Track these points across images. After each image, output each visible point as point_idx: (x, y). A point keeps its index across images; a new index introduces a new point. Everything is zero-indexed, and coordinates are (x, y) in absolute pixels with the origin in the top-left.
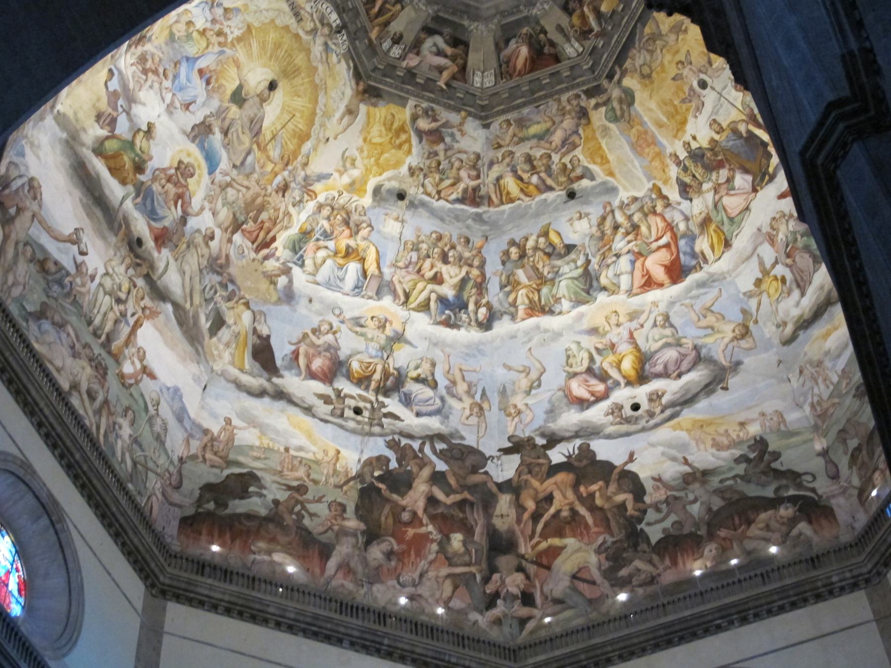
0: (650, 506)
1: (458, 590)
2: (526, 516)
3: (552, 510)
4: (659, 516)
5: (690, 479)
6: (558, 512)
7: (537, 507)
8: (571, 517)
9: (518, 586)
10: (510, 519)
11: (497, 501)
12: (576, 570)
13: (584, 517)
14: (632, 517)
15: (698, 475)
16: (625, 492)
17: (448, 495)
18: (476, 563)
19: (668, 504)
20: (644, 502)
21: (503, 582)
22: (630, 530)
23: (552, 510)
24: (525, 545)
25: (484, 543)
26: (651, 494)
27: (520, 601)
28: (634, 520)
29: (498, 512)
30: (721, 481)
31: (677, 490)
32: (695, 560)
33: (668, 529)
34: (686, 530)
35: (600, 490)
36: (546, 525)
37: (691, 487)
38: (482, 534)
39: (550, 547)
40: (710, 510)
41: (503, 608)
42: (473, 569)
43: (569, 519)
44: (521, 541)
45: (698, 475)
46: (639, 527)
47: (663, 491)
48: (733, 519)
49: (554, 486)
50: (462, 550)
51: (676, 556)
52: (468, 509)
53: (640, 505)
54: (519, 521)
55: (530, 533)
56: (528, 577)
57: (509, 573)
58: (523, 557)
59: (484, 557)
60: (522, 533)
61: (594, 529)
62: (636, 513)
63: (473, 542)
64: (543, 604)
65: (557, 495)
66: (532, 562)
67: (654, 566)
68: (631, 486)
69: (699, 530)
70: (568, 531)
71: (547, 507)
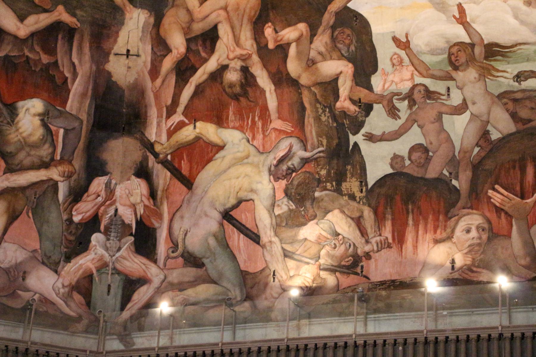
0: (380, 99)
1: (16, 224)
2: (168, 63)
3: (212, 65)
4: (393, 125)
5: (463, 58)
6: (224, 68)
7: (188, 49)
8: (242, 86)
9: (133, 206)
10: (140, 61)
11: (122, 23)
12: (232, 201)
13: (263, 92)
14: (344, 113)
15: (478, 50)
16: (342, 57)
17: (22, 18)
18: (62, 161)
19: (412, 103)
20: (370, 88)
21: (110, 191)
22: (335, 142)
23: (212, 65)
24: (159, 125)
25: (84, 117)
26: (385, 74)
27: (132, 239)
28: (346, 122)
29: (120, 46)
30: (519, 77)
31: (433, 77)
32: (437, 242)
33: (403, 158)
34: (432, 173)
35: (298, 40)
36: (199, 91)
37: (459, 75)
38: (83, 95)
39: (198, 139)
40: (485, 134)
41: (101, 251)
42: (54, 173)
43: (238, 89)
44: (153, 113)
45: (478, 50)
46: (353, 139)
47: (407, 72)
48: (523, 170)
49: (222, 13)
50: (40, 132)
51: (406, 224)
52: (61, 46)
53: (362, 93)
54: (154, 72)
55: (169, 102)
56: (153, 194)
57: (124, 178)
58: (150, 146)
59: (81, 145)
60: (157, 96)
61: (277, 124)
62: (353, 108)
63: (63, 114)
64: (168, 257)
65: (224, 31)
66: (165, 163)
67: (363, 232)
68: (353, 48)
69: (457, 178)
70: (231, 116)
71: (203, 54)
